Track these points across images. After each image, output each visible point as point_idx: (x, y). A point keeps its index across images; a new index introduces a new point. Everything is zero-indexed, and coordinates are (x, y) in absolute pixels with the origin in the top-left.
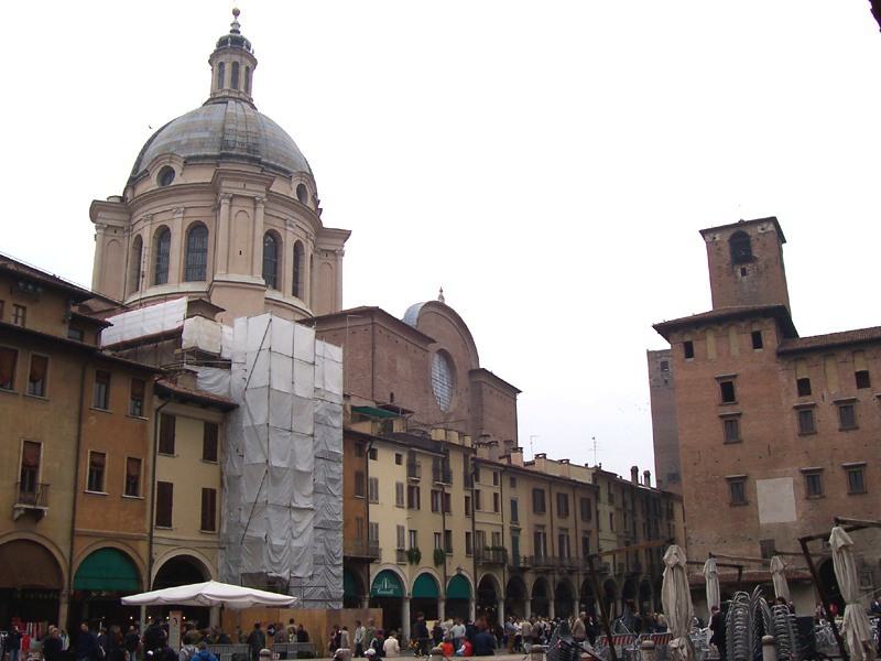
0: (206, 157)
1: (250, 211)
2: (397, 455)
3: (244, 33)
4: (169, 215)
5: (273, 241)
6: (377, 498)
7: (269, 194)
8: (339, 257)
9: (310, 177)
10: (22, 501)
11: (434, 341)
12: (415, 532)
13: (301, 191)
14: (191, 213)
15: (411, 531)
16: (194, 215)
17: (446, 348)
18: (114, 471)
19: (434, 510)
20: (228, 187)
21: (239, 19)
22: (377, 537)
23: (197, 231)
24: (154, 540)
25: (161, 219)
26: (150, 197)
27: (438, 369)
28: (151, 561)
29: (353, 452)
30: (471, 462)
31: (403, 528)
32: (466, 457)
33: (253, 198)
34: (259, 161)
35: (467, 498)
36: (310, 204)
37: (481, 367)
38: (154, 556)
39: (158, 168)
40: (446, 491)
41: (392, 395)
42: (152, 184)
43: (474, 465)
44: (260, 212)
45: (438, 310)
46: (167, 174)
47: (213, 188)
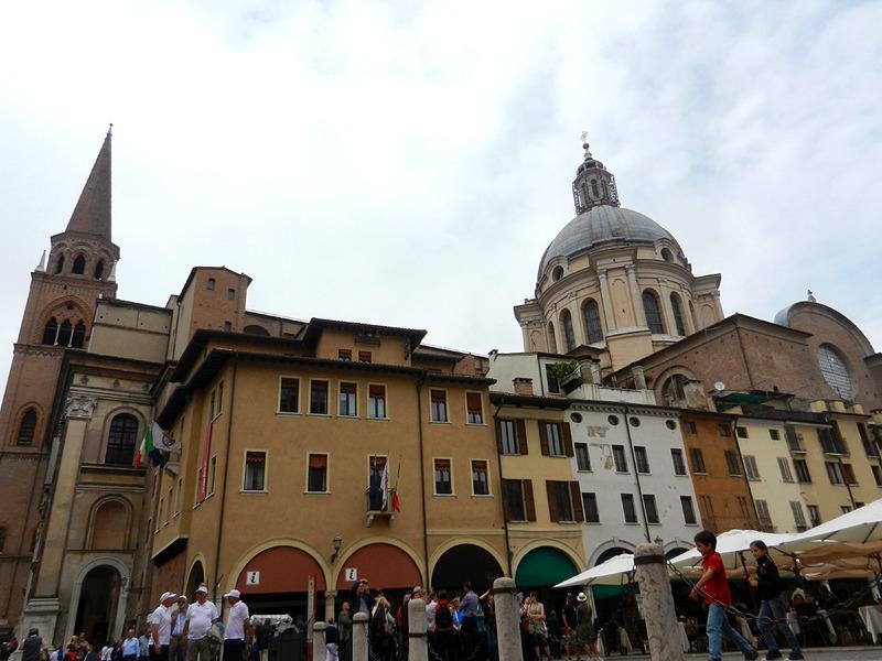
0: (582, 250)
1: (624, 278)
2: (771, 431)
3: (594, 158)
4: (564, 302)
5: (650, 296)
6: (757, 475)
7: (635, 261)
8: (716, 298)
9: (673, 242)
10: (372, 509)
11: (810, 335)
12: (815, 507)
13: (665, 253)
14: (581, 294)
15: (809, 506)
16: (584, 294)
17: (829, 341)
18: (462, 477)
19: (834, 481)
20: (602, 264)
21: (590, 150)
22: (767, 512)
23: (590, 306)
24: (509, 534)
25: (561, 306)
26: (552, 291)
27: (827, 362)
28: (510, 556)
29: (719, 433)
30: (868, 431)
31: (798, 503)
32: (861, 427)
33: (623, 268)
34: (623, 240)
35: (875, 469)
36: (676, 261)
37: (876, 352)
38: (512, 550)
39: (553, 273)
40: (844, 461)
41: (776, 388)
42: (551, 281)
43: (873, 432)
44: (632, 276)
45: (808, 307)
46: (559, 271)
47: (592, 271)
